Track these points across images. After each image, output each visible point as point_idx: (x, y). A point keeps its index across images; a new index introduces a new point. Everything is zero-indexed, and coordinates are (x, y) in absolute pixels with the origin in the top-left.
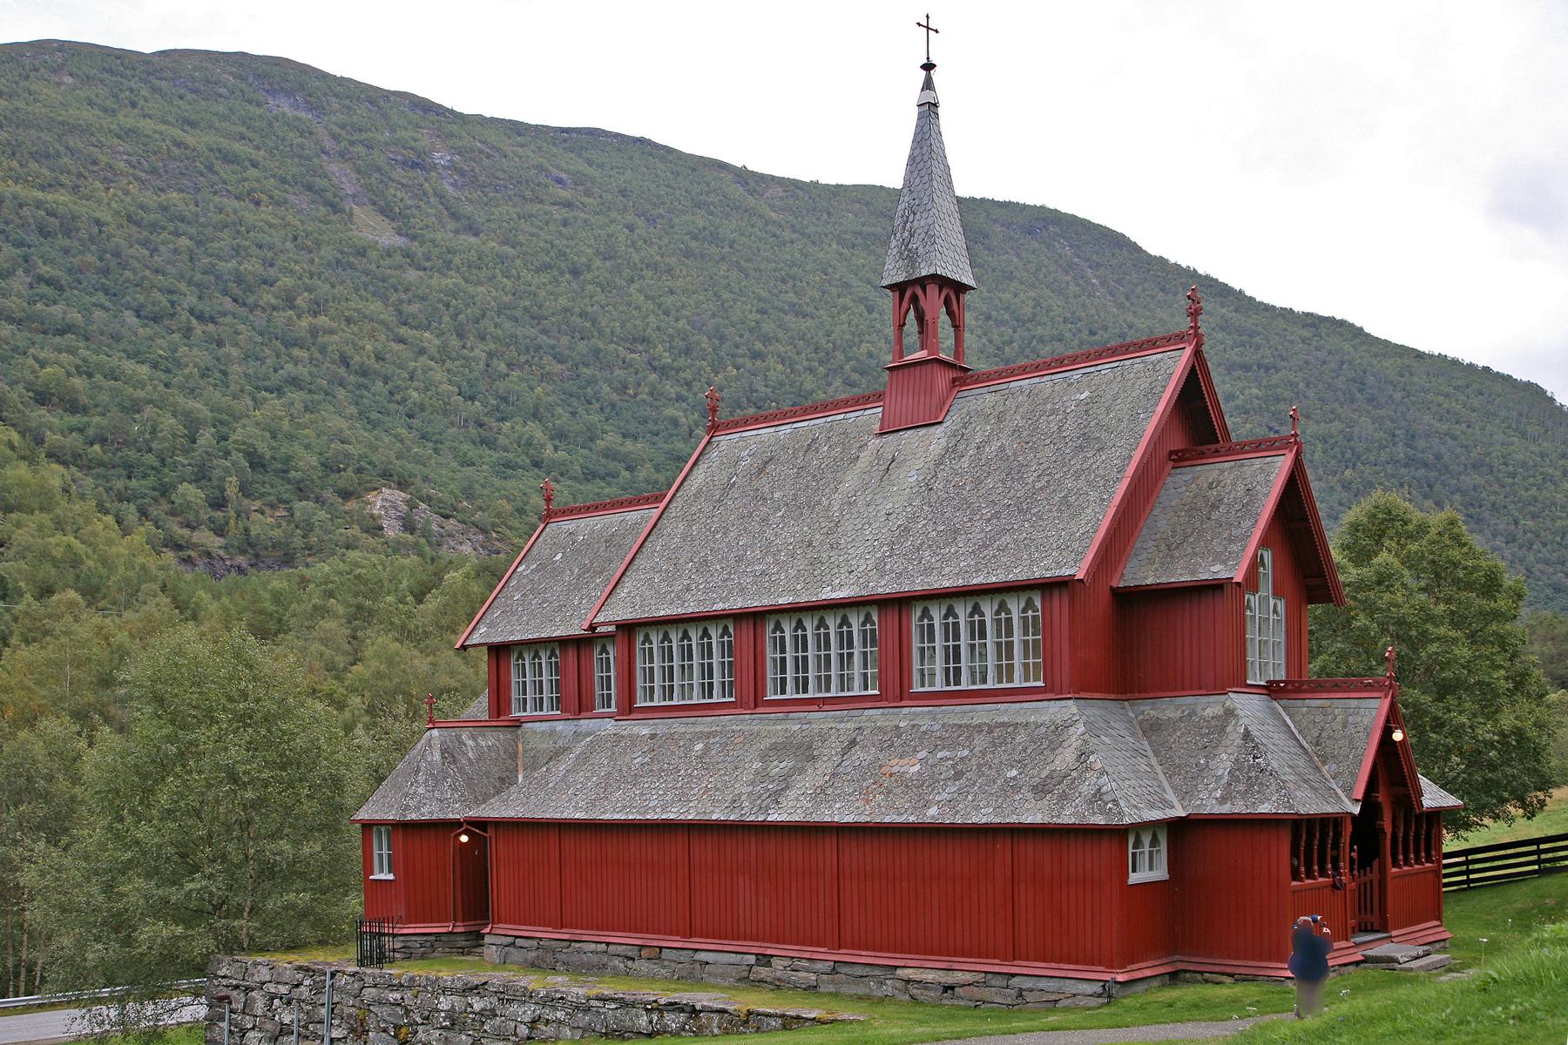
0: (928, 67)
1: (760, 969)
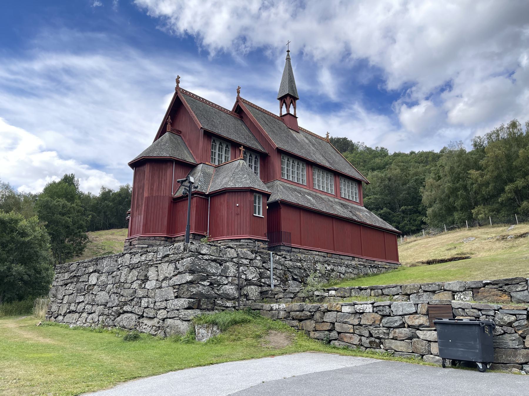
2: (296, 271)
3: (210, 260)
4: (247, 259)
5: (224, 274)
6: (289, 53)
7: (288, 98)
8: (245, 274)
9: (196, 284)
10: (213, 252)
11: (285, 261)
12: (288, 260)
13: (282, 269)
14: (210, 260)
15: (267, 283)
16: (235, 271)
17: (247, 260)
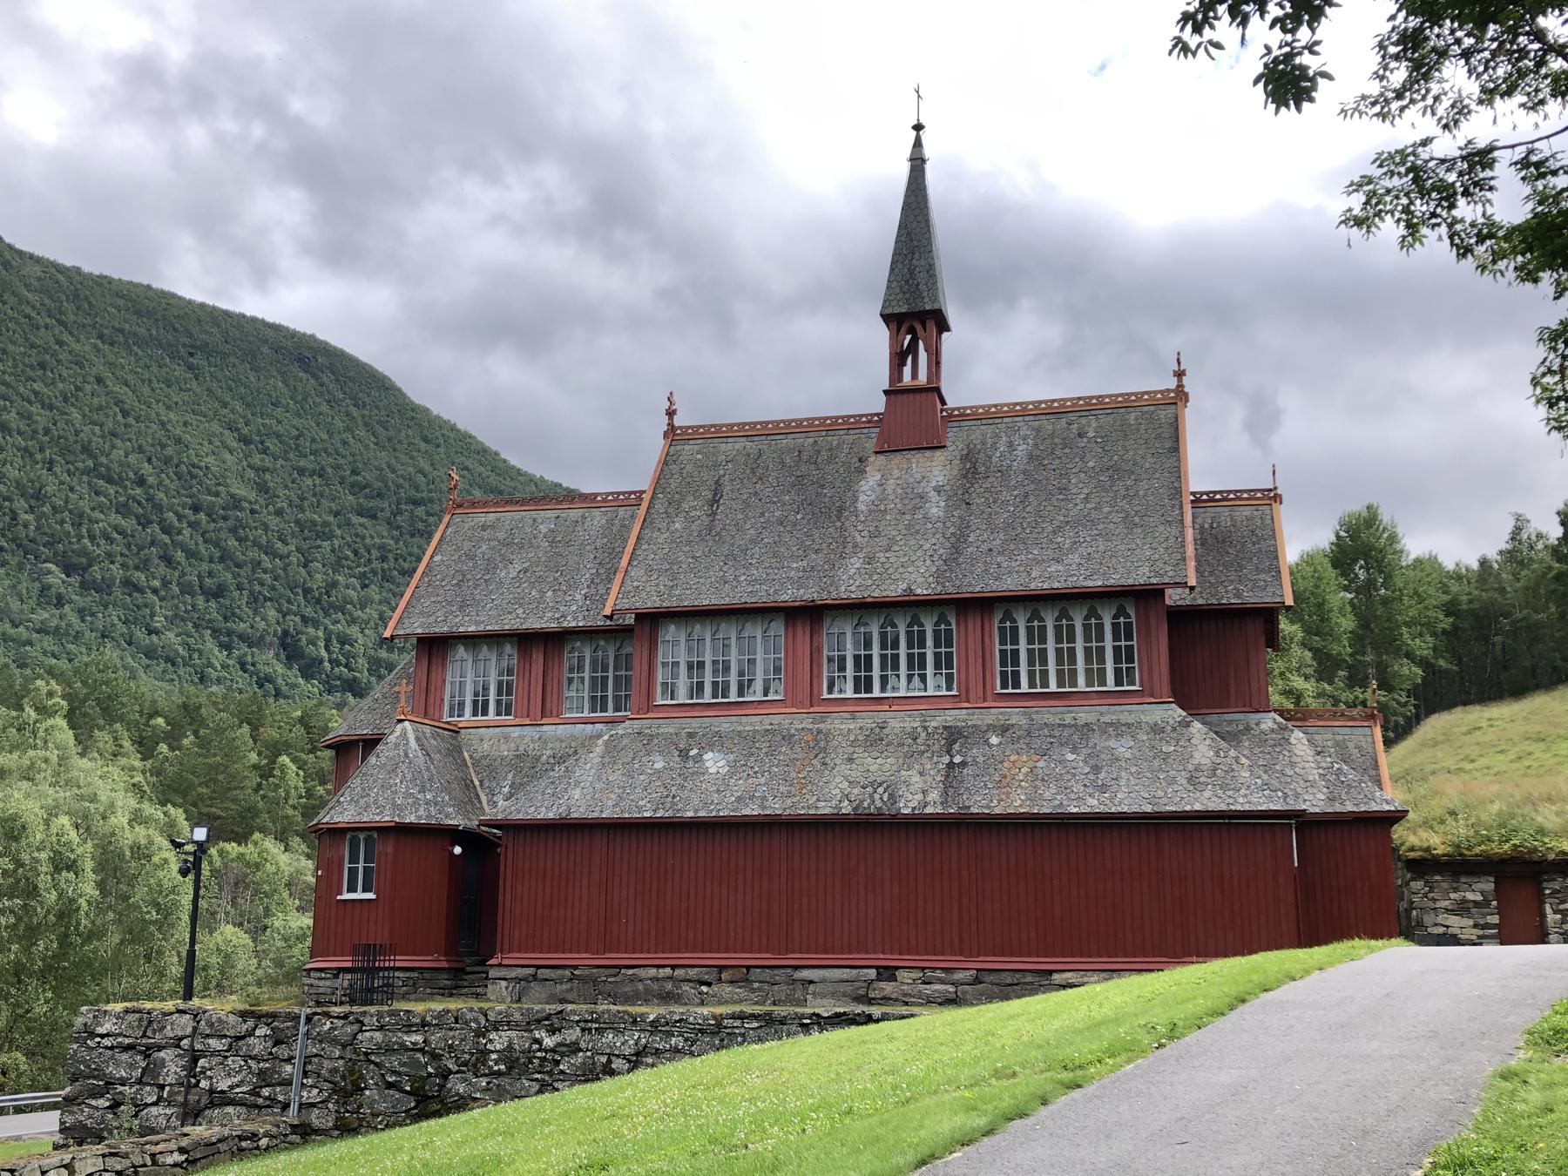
0: (918, 127)
1: (882, 984)
2: (394, 1062)
3: (117, 1047)
4: (225, 1036)
5: (150, 1075)
6: (921, 133)
8: (211, 1078)
9: (79, 1104)
10: (130, 1026)
11: (361, 1031)
12: (368, 1028)
13: (342, 1058)
14: (117, 1047)
15: (281, 1098)
16: (178, 1070)
17: (224, 1041)
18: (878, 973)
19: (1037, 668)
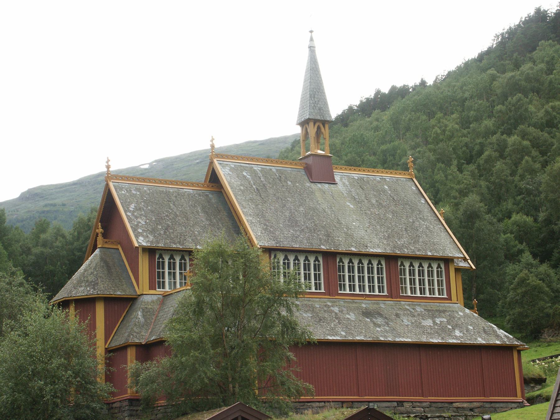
6: (312, 33)
7: (311, 124)
18: (398, 404)
19: (362, 284)
